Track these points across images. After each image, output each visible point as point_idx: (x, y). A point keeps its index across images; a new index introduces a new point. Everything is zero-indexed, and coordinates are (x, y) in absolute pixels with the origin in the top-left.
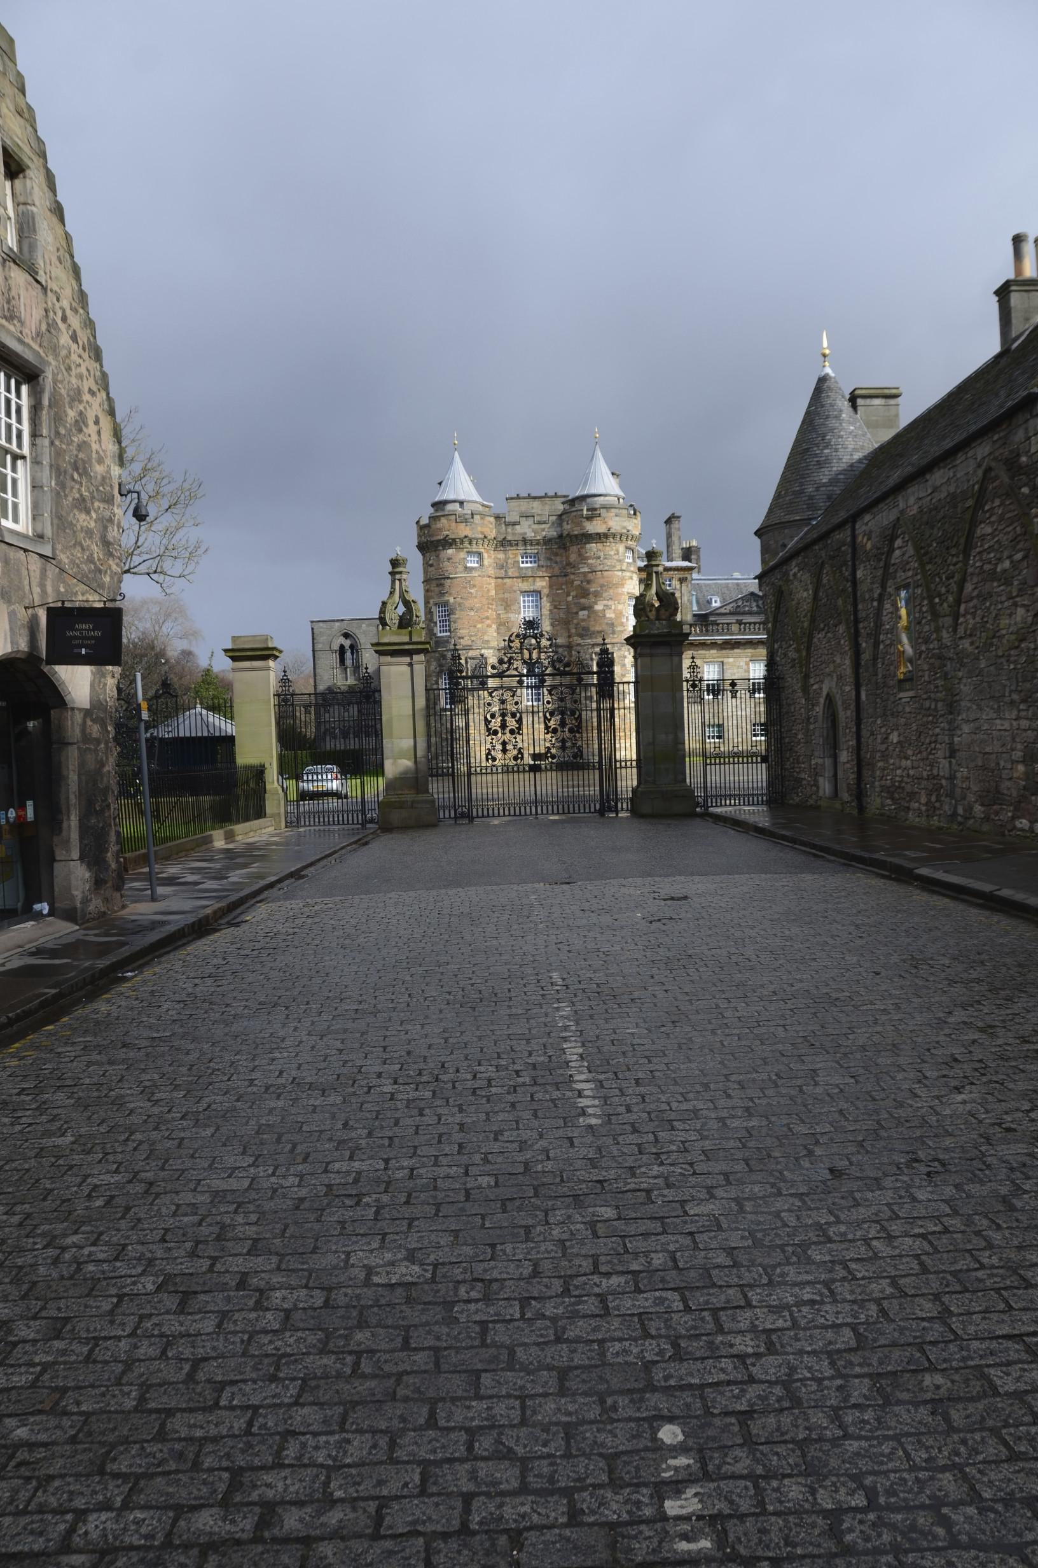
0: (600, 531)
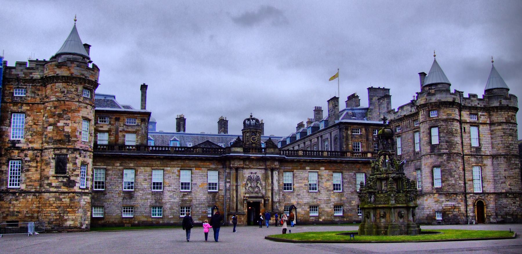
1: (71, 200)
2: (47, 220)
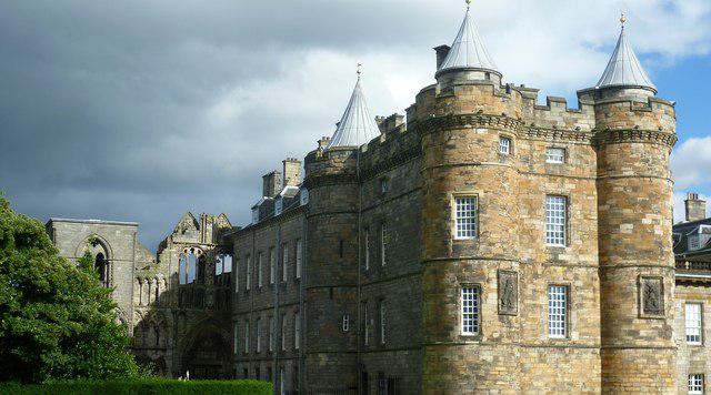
0: (651, 129)
1: (669, 362)
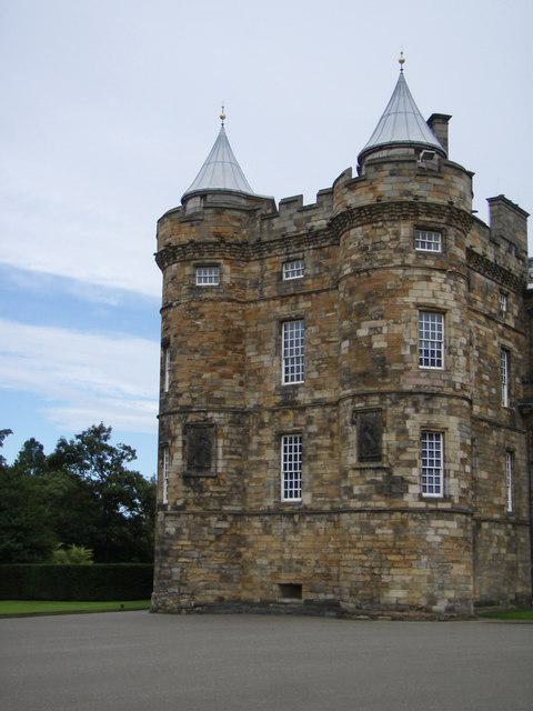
1: (397, 531)
2: (346, 584)
